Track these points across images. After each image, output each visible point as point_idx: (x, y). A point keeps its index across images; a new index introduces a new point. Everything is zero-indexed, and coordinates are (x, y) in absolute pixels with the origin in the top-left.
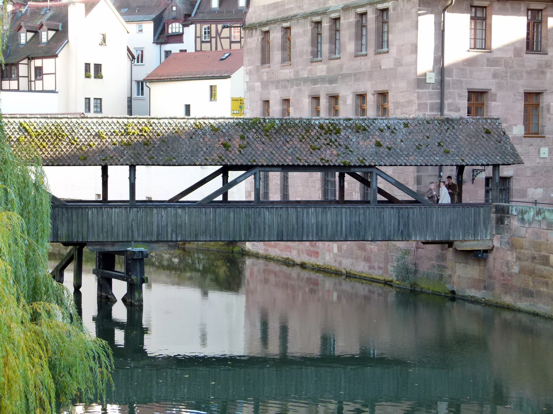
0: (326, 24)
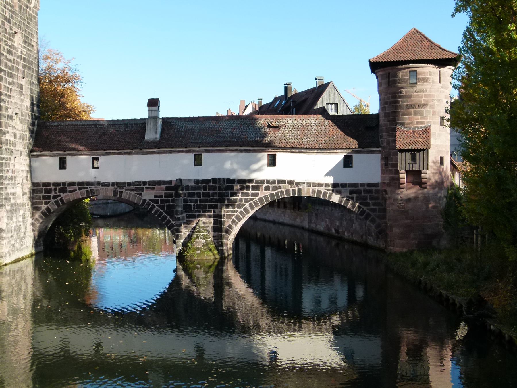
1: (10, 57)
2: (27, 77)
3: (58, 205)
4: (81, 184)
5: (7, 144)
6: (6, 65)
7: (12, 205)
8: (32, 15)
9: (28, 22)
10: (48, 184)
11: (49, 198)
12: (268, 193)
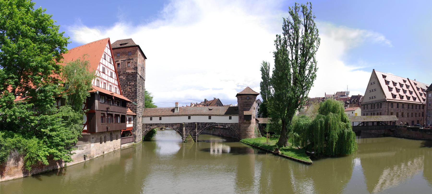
0: (373, 105)
1: (139, 92)
6: (138, 95)
10: (147, 124)
11: (147, 127)
12: (209, 126)
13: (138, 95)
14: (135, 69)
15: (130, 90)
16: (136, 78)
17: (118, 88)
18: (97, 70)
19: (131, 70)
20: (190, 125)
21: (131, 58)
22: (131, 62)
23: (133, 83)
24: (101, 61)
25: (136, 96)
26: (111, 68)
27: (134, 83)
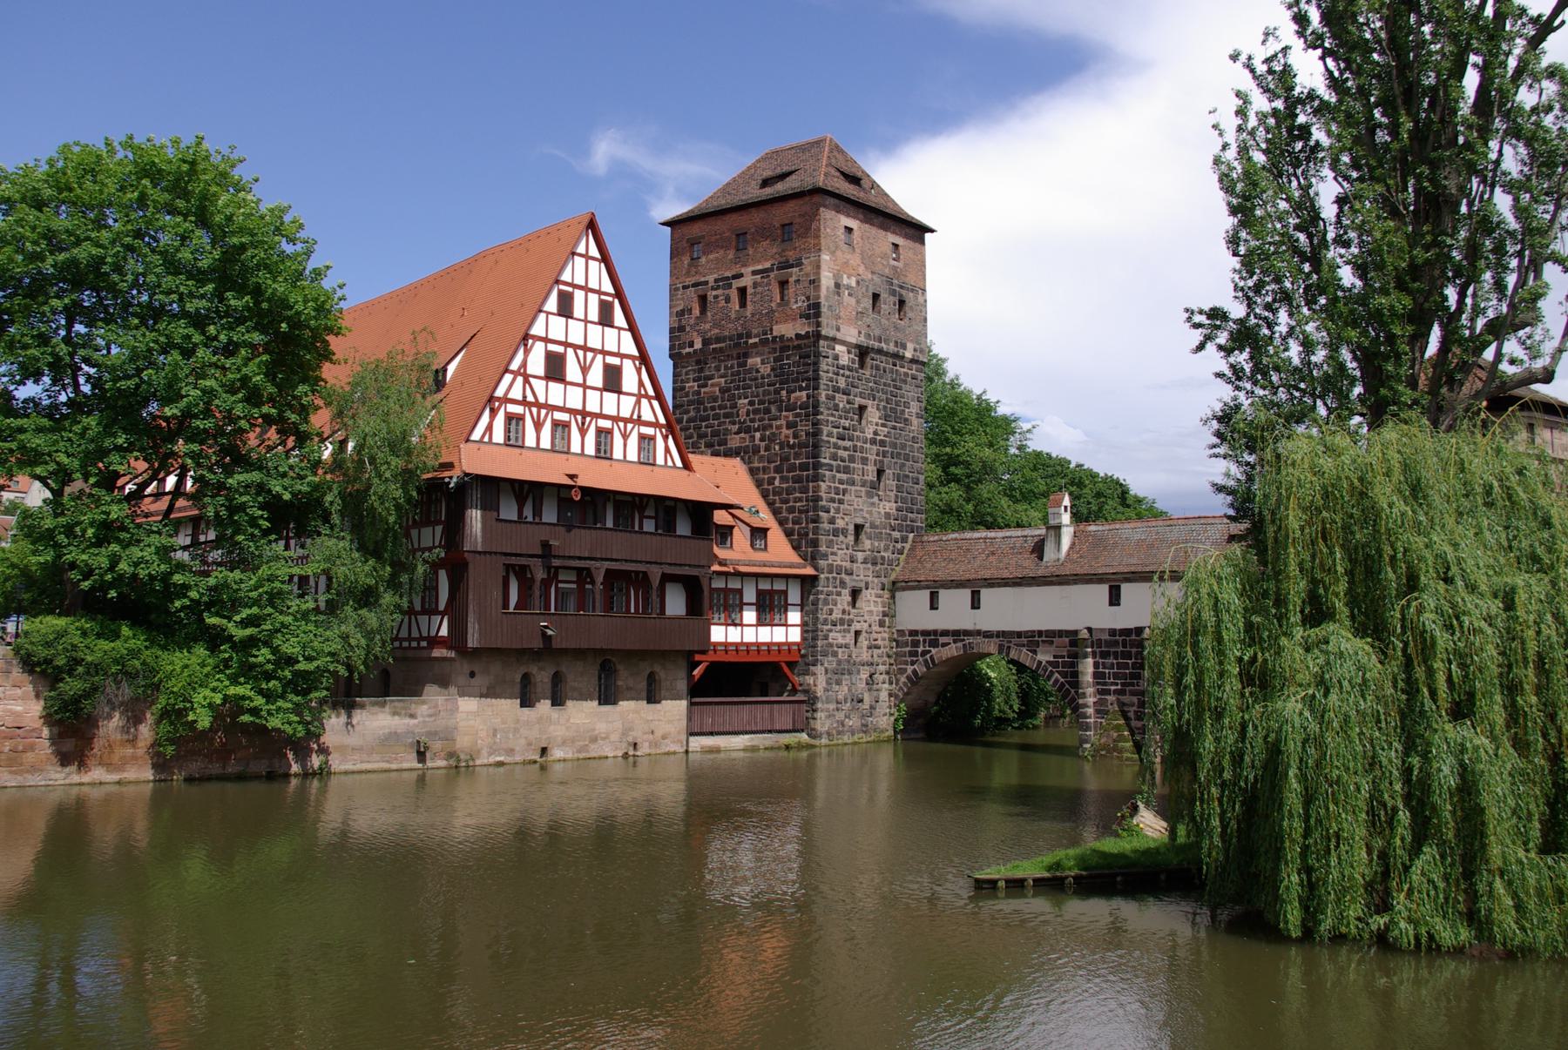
2: (890, 468)
3: (928, 668)
4: (957, 634)
5: (830, 572)
6: (834, 457)
7: (839, 662)
8: (906, 374)
9: (895, 387)
13: (834, 457)
14: (808, 317)
15: (790, 432)
16: (816, 364)
17: (665, 438)
18: (512, 372)
19: (794, 319)
20: (1116, 643)
21: (791, 255)
22: (792, 280)
23: (804, 393)
24: (538, 329)
25: (817, 466)
26: (611, 346)
27: (808, 397)
